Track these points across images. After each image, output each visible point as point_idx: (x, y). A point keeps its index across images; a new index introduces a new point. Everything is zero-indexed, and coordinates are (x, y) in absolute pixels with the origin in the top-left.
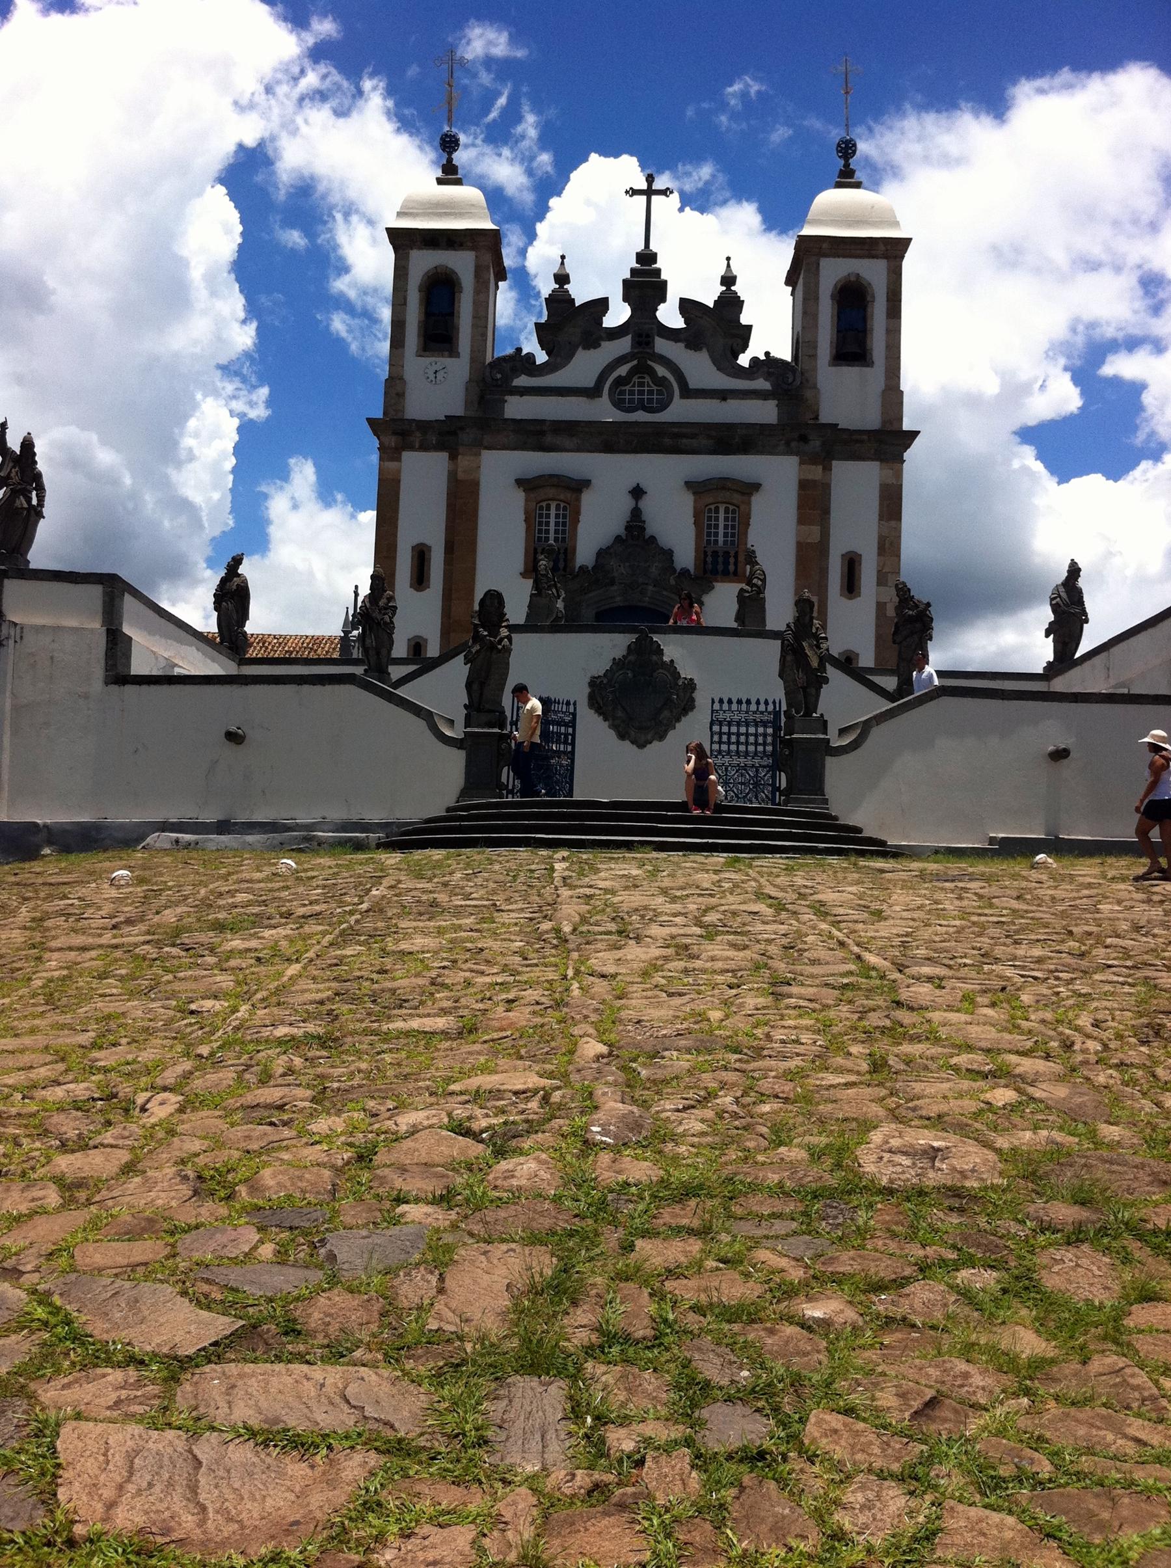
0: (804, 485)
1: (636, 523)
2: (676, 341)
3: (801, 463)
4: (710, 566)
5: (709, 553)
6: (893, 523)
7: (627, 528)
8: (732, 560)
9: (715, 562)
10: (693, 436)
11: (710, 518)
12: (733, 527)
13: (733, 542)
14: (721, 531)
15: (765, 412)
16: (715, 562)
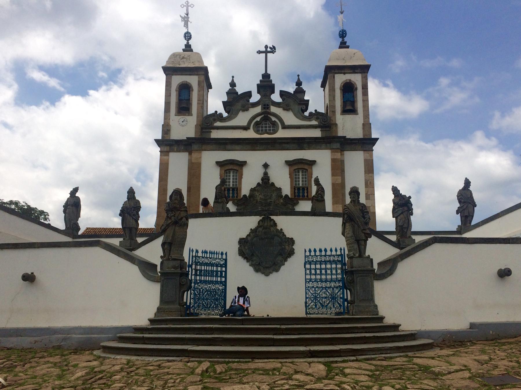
0: (333, 161)
1: (266, 178)
2: (279, 107)
3: (331, 152)
4: (297, 194)
5: (296, 189)
6: (370, 175)
7: (262, 179)
8: (306, 191)
9: (299, 193)
10: (288, 143)
11: (296, 175)
12: (306, 178)
13: (306, 184)
14: (301, 180)
15: (317, 133)
16: (299, 193)
